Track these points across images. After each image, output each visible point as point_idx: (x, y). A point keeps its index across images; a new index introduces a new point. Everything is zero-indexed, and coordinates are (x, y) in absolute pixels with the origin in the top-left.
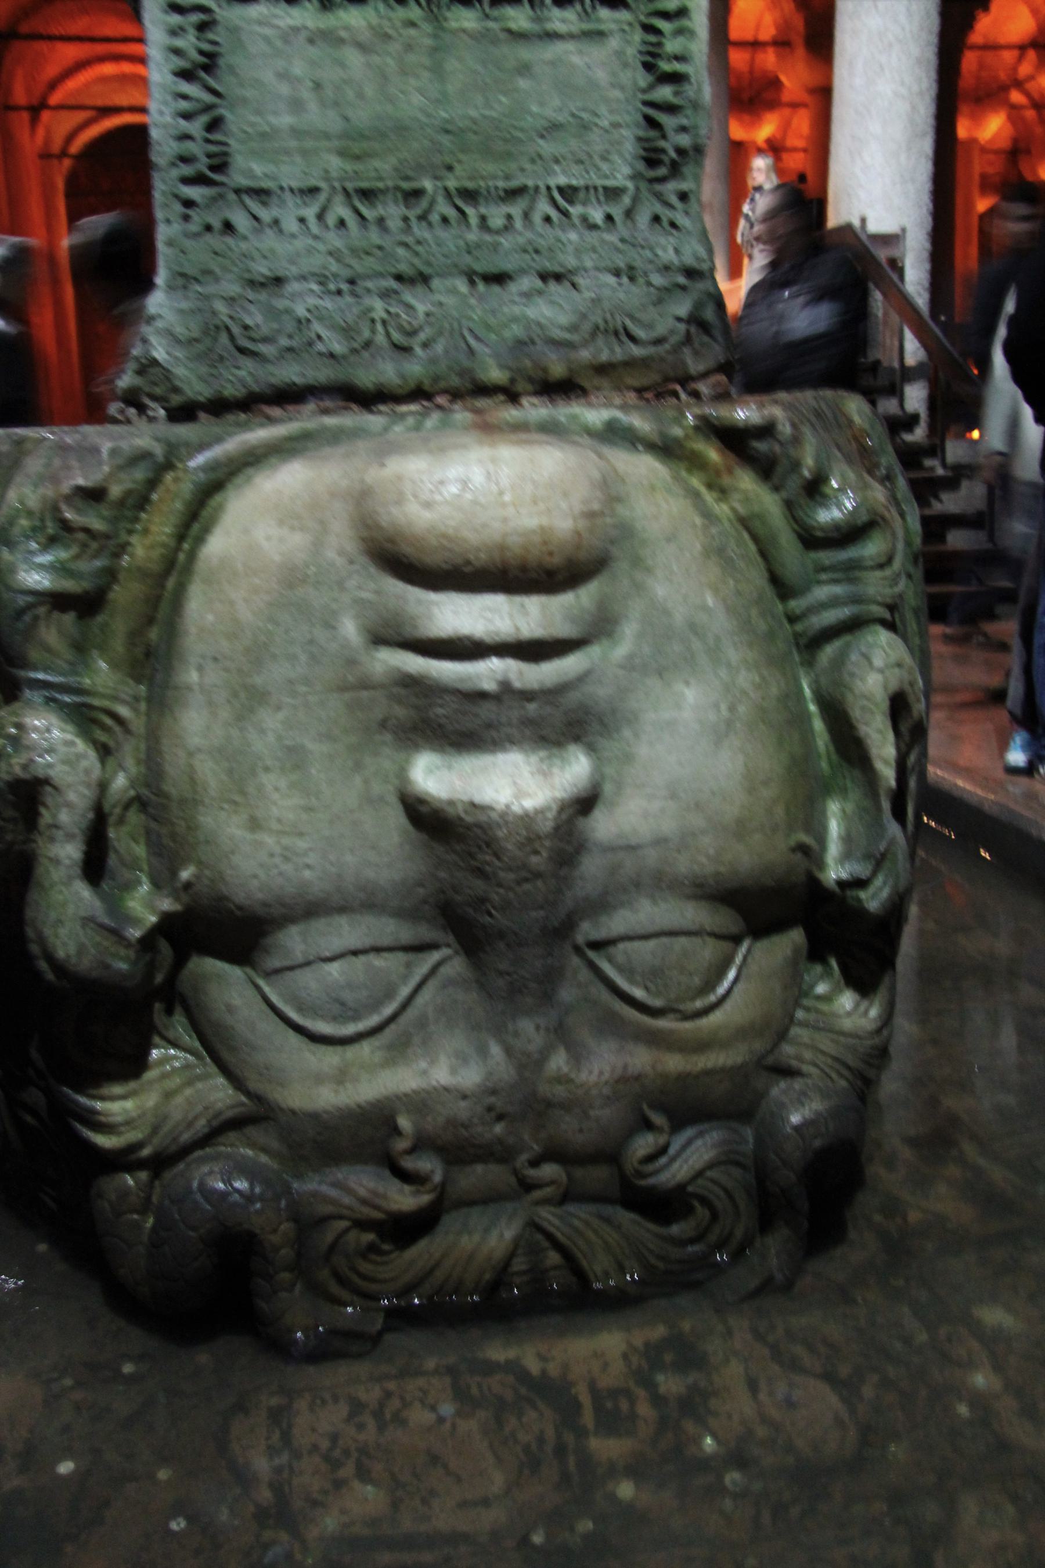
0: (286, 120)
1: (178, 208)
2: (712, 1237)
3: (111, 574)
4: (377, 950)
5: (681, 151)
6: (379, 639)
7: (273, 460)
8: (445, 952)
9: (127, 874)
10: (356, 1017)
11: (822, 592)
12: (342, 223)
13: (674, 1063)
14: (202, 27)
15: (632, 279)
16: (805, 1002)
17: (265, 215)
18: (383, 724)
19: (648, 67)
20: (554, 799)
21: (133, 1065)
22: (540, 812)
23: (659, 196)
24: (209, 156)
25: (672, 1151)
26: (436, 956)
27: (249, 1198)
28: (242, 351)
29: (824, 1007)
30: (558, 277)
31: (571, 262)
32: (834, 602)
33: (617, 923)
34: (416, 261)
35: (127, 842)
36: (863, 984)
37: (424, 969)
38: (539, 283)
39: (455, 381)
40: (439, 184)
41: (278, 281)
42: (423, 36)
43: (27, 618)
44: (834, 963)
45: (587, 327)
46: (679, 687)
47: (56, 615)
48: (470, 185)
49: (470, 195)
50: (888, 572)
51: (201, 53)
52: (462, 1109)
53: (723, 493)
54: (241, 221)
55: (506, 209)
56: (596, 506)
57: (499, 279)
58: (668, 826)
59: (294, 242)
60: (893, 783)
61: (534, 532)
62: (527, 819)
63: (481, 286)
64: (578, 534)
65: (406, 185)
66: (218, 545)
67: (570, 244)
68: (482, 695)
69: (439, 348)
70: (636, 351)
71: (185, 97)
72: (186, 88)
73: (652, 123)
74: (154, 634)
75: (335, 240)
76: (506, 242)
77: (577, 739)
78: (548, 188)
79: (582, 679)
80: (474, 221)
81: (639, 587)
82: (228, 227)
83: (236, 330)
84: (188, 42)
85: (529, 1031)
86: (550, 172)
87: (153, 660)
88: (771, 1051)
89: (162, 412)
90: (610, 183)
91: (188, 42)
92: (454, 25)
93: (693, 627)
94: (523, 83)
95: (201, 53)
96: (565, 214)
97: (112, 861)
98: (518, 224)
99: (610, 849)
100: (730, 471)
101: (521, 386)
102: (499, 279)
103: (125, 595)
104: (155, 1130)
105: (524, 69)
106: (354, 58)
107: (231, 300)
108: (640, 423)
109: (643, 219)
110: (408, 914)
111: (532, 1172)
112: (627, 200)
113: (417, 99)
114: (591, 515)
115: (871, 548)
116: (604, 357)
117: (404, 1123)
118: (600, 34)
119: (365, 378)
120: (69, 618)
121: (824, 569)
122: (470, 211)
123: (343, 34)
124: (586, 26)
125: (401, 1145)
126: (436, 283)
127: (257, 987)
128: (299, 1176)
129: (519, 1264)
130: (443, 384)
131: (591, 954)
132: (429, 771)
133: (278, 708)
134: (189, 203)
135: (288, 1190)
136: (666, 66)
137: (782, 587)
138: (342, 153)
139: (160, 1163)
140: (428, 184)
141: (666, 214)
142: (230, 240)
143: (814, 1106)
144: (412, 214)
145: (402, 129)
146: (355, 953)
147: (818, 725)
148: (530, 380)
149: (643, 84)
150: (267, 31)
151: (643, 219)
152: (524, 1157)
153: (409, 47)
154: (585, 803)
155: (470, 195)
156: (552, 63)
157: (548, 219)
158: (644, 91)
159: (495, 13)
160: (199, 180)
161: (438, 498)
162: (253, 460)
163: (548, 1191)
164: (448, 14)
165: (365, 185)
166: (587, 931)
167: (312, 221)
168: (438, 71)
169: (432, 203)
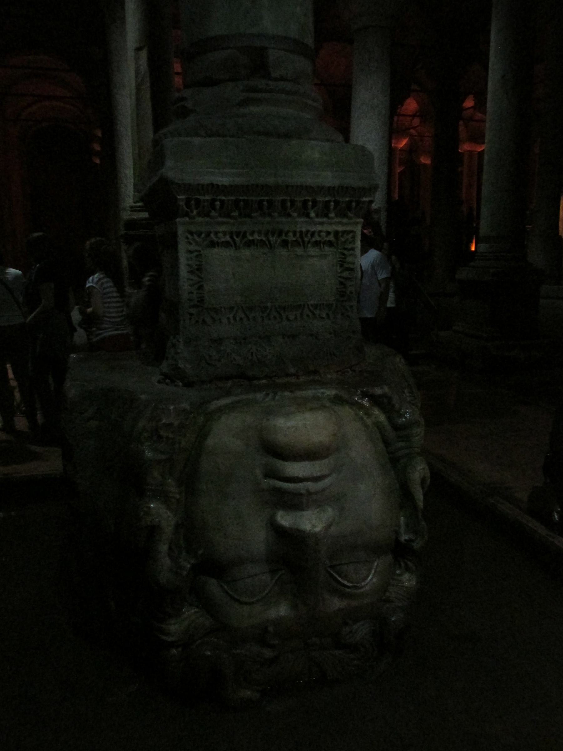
6: (267, 476)
8: (283, 572)
12: (241, 319)
13: (354, 603)
19: (341, 266)
22: (320, 531)
26: (280, 573)
28: (209, 364)
29: (400, 578)
51: (196, 265)
54: (208, 320)
66: (210, 442)
71: (192, 280)
72: (192, 277)
78: (308, 305)
82: (204, 322)
95: (196, 265)
96: (313, 313)
114: (335, 435)
117: (271, 629)
118: (325, 256)
122: (282, 313)
127: (221, 586)
132: (282, 517)
133: (234, 499)
134: (191, 314)
136: (346, 266)
140: (269, 304)
144: (265, 315)
149: (339, 271)
157: (308, 316)
158: (339, 273)
161: (288, 433)
167: (232, 319)
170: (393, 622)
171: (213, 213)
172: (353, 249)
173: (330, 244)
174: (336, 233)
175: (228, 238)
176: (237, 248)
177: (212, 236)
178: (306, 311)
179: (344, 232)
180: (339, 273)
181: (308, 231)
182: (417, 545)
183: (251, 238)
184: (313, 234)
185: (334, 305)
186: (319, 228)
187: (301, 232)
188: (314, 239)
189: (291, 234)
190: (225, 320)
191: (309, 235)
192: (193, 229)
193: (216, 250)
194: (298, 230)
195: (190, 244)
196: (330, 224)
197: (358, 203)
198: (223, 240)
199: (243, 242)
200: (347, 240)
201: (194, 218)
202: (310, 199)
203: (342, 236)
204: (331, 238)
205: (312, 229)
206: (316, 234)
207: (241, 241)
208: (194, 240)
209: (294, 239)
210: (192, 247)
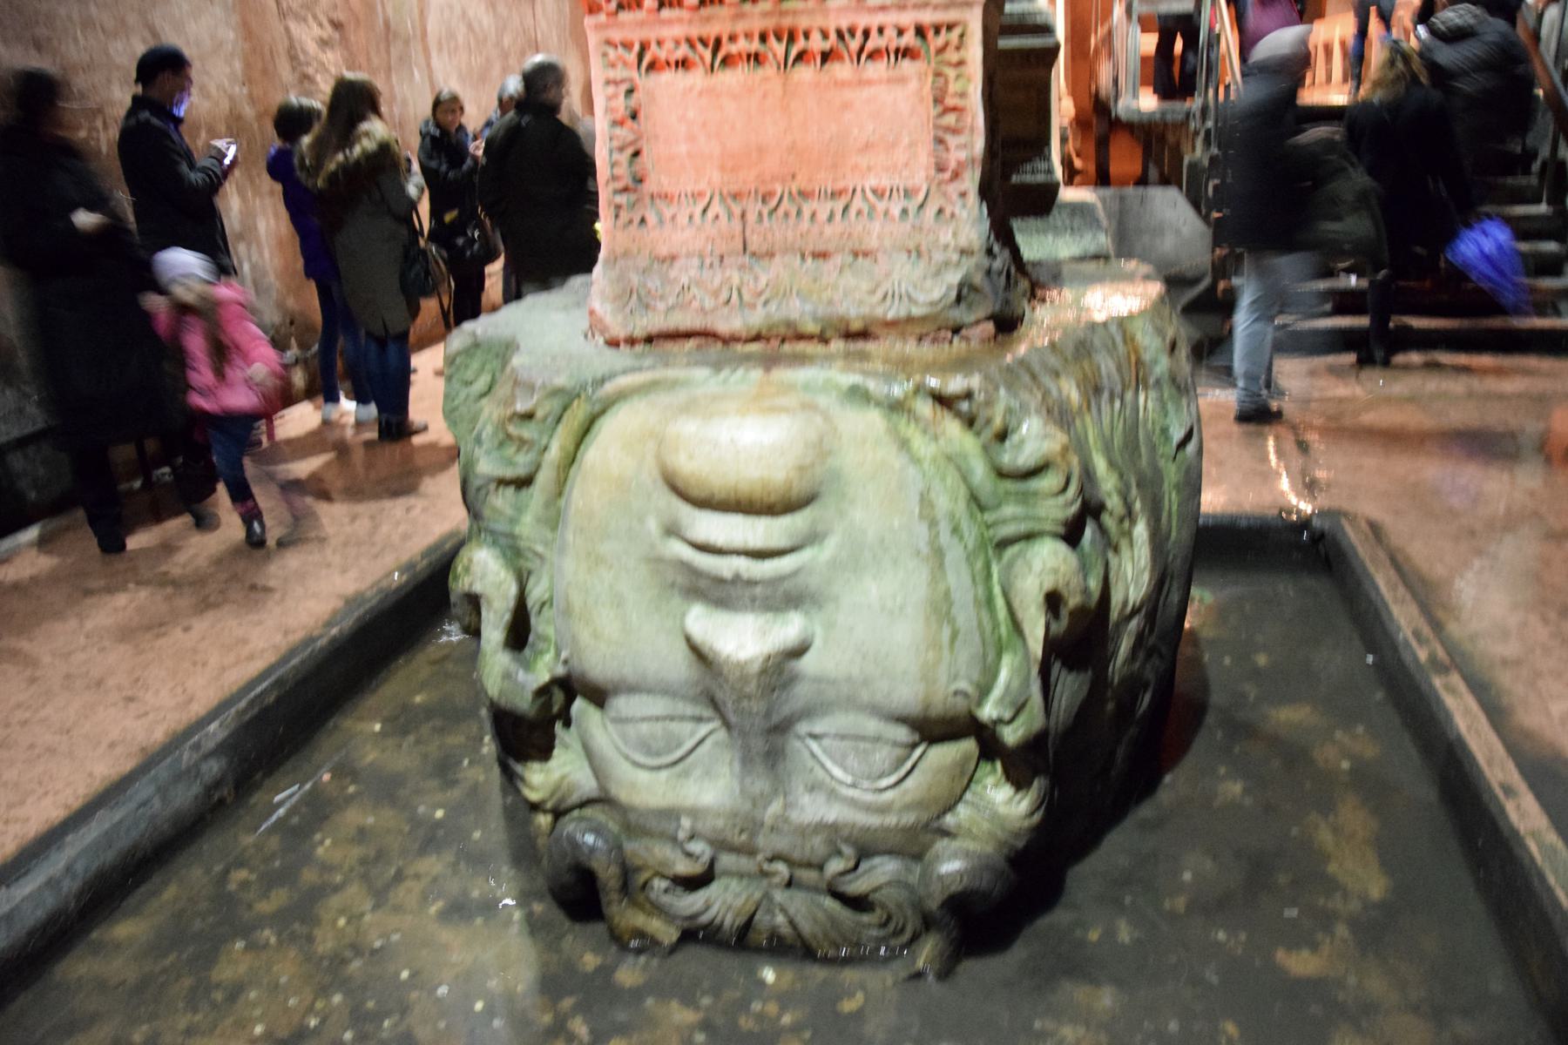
0: (683, 148)
2: (891, 927)
3: (538, 467)
4: (672, 718)
7: (636, 398)
9: (541, 645)
10: (658, 754)
11: (1009, 510)
12: (717, 217)
14: (630, 92)
19: (938, 100)
21: (544, 752)
23: (945, 194)
27: (592, 849)
30: (866, 255)
31: (873, 243)
32: (1014, 519)
35: (541, 625)
36: (1018, 781)
39: (782, 330)
41: (673, 258)
42: (776, 84)
43: (483, 492)
44: (999, 765)
45: (879, 294)
48: (809, 188)
49: (805, 195)
50: (1061, 500)
52: (720, 823)
53: (936, 438)
54: (652, 218)
55: (829, 205)
56: (808, 461)
57: (822, 255)
58: (855, 671)
59: (682, 232)
62: (742, 666)
67: (875, 233)
69: (773, 307)
70: (917, 311)
72: (618, 131)
74: (562, 502)
75: (711, 230)
76: (828, 230)
77: (796, 607)
79: (795, 573)
82: (643, 220)
83: (643, 293)
85: (760, 785)
87: (554, 519)
88: (938, 817)
89: (601, 341)
90: (910, 184)
96: (872, 208)
98: (838, 216)
99: (818, 680)
101: (828, 334)
102: (822, 255)
103: (544, 478)
104: (552, 795)
105: (846, 106)
108: (872, 385)
109: (930, 211)
110: (694, 700)
111: (766, 866)
115: (1049, 482)
116: (890, 315)
117: (686, 823)
118: (902, 80)
119: (723, 327)
120: (510, 490)
126: (777, 259)
128: (629, 838)
130: (774, 332)
134: (618, 207)
135: (620, 848)
136: (950, 101)
137: (976, 502)
138: (722, 168)
139: (558, 814)
142: (644, 230)
145: (761, 150)
146: (657, 719)
147: (1000, 602)
148: (837, 330)
151: (930, 211)
152: (760, 857)
154: (798, 651)
155: (805, 195)
160: (625, 190)
162: (621, 396)
166: (803, 728)
170: (940, 878)
174: (920, 31)
175: (683, 51)
177: (654, 46)
178: (858, 203)
182: (1011, 735)
188: (870, 45)
189: (816, 37)
190: (683, 219)
192: (617, 35)
193: (667, 77)
195: (613, 65)
204: (909, 39)
206: (874, 33)
208: (621, 58)
209: (826, 46)
210: (619, 73)
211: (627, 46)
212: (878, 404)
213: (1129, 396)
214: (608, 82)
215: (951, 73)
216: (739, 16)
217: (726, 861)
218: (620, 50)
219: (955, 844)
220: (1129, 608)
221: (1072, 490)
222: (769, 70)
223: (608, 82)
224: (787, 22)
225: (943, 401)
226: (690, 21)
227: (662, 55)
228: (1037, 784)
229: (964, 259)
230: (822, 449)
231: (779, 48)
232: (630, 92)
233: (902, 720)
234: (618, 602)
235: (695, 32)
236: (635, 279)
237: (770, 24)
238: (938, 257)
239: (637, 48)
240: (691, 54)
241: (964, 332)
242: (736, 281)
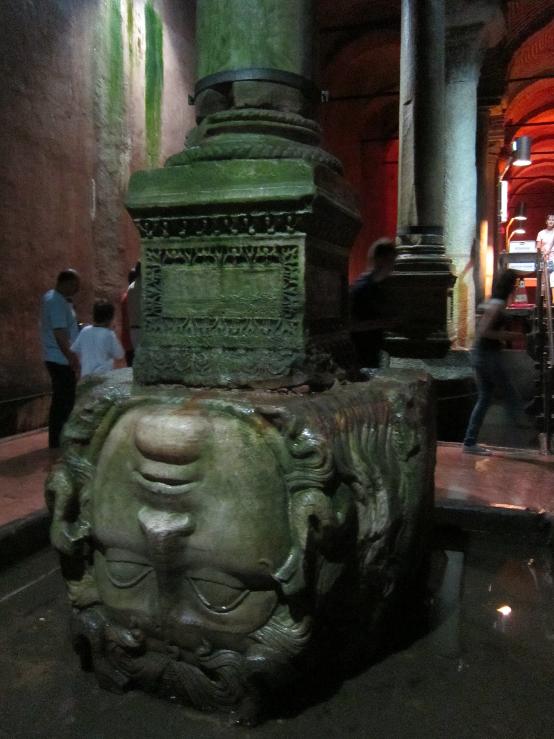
1: (145, 323)
5: (295, 309)
8: (152, 568)
11: (295, 474)
12: (190, 329)
13: (213, 625)
14: (157, 271)
15: (275, 351)
16: (273, 617)
17: (170, 325)
18: (135, 495)
19: (286, 281)
20: (165, 530)
22: (159, 534)
23: (289, 323)
24: (156, 308)
25: (212, 656)
30: (252, 350)
33: (199, 574)
34: (208, 342)
36: (297, 619)
37: (145, 572)
38: (243, 352)
39: (212, 383)
40: (220, 317)
41: (170, 346)
45: (256, 368)
46: (221, 502)
47: (74, 444)
48: (229, 318)
49: (229, 322)
51: (155, 279)
52: (147, 619)
54: (162, 327)
57: (234, 349)
60: (304, 548)
61: (170, 446)
63: (227, 351)
64: (185, 447)
65: (210, 318)
68: (153, 493)
71: (150, 291)
72: (152, 289)
73: (286, 299)
77: (188, 511)
79: (187, 493)
80: (228, 330)
81: (212, 467)
82: (158, 329)
84: (152, 276)
86: (254, 315)
88: (253, 632)
91: (152, 276)
92: (227, 269)
93: (229, 482)
94: (248, 287)
95: (155, 279)
97: (80, 517)
98: (241, 331)
100: (265, 428)
103: (95, 441)
104: (79, 599)
106: (198, 280)
107: (155, 352)
108: (238, 408)
112: (278, 325)
113: (216, 291)
115: (316, 460)
118: (271, 271)
120: (78, 445)
121: (296, 466)
123: (195, 272)
124: (267, 268)
125: (131, 625)
126: (213, 350)
129: (166, 677)
130: (208, 383)
131: (193, 582)
134: (149, 322)
136: (291, 282)
140: (217, 318)
141: (290, 330)
142: (158, 334)
143: (259, 658)
149: (284, 287)
150: (174, 272)
153: (214, 276)
154: (187, 532)
155: (229, 322)
156: (257, 280)
158: (284, 289)
159: (239, 265)
163: (173, 655)
164: (225, 266)
165: (198, 317)
166: (189, 574)
167: (181, 328)
168: (222, 284)
169: (217, 324)
171: (165, 232)
172: (296, 264)
173: (274, 259)
174: (279, 249)
175: (180, 255)
176: (191, 264)
177: (167, 253)
178: (250, 327)
179: (286, 248)
180: (284, 289)
181: (250, 248)
182: (286, 588)
183: (200, 255)
184: (256, 248)
185: (279, 322)
186: (261, 243)
187: (244, 248)
188: (257, 255)
189: (234, 250)
190: (175, 329)
191: (252, 250)
192: (153, 247)
194: (242, 246)
195: (150, 260)
196: (271, 239)
197: (295, 216)
198: (177, 256)
199: (195, 258)
200: (291, 255)
201: (150, 238)
202: (244, 215)
203: (286, 251)
204: (274, 253)
205: (254, 244)
206: (259, 250)
207: (193, 256)
208: (153, 257)
209: (238, 255)
211: (156, 251)
212: (238, 417)
213: (381, 427)
214: (148, 267)
215: (291, 268)
216: (203, 241)
217: (152, 643)
218: (154, 254)
219: (260, 647)
220: (372, 535)
221: (327, 466)
222: (215, 266)
223: (148, 267)
224: (223, 243)
225: (270, 418)
226: (182, 242)
227: (170, 256)
228: (307, 619)
229: (294, 354)
230: (204, 434)
231: (219, 255)
232: (157, 271)
233: (235, 574)
234: (112, 500)
235: (185, 246)
236: (151, 354)
237: (214, 244)
238: (283, 353)
239: (160, 253)
240: (182, 256)
241: (294, 389)
242: (193, 359)
